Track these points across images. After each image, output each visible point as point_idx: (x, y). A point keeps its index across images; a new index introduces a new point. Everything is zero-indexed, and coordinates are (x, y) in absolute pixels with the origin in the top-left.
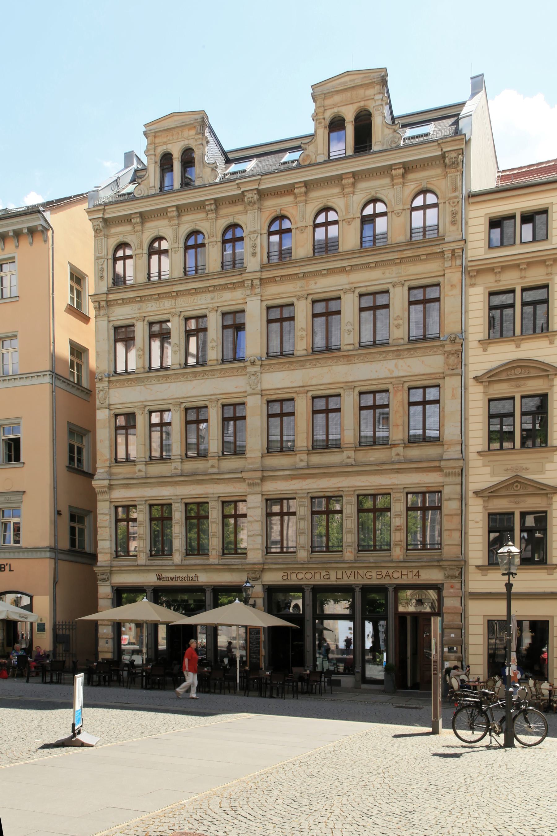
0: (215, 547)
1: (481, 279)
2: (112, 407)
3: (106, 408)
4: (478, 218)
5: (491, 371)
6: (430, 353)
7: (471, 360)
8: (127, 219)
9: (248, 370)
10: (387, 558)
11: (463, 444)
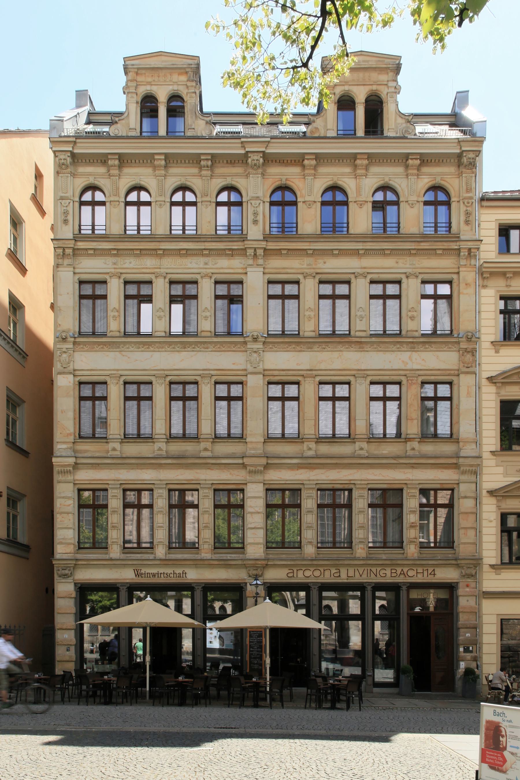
0: (208, 540)
1: (491, 283)
2: (77, 373)
3: (70, 373)
4: (489, 222)
5: (504, 372)
6: (445, 349)
7: (484, 360)
8: (102, 160)
9: (249, 346)
10: (401, 556)
11: (477, 443)
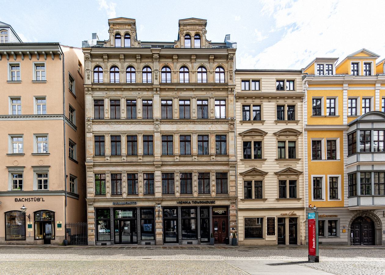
3: (91, 132)
7: (237, 127)
8: (101, 56)
10: (209, 196)
11: (235, 156)
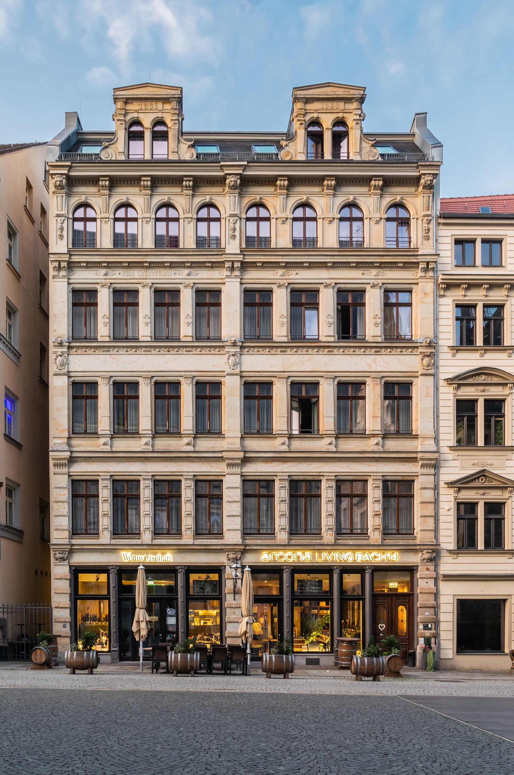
2: (72, 374)
3: (64, 375)
